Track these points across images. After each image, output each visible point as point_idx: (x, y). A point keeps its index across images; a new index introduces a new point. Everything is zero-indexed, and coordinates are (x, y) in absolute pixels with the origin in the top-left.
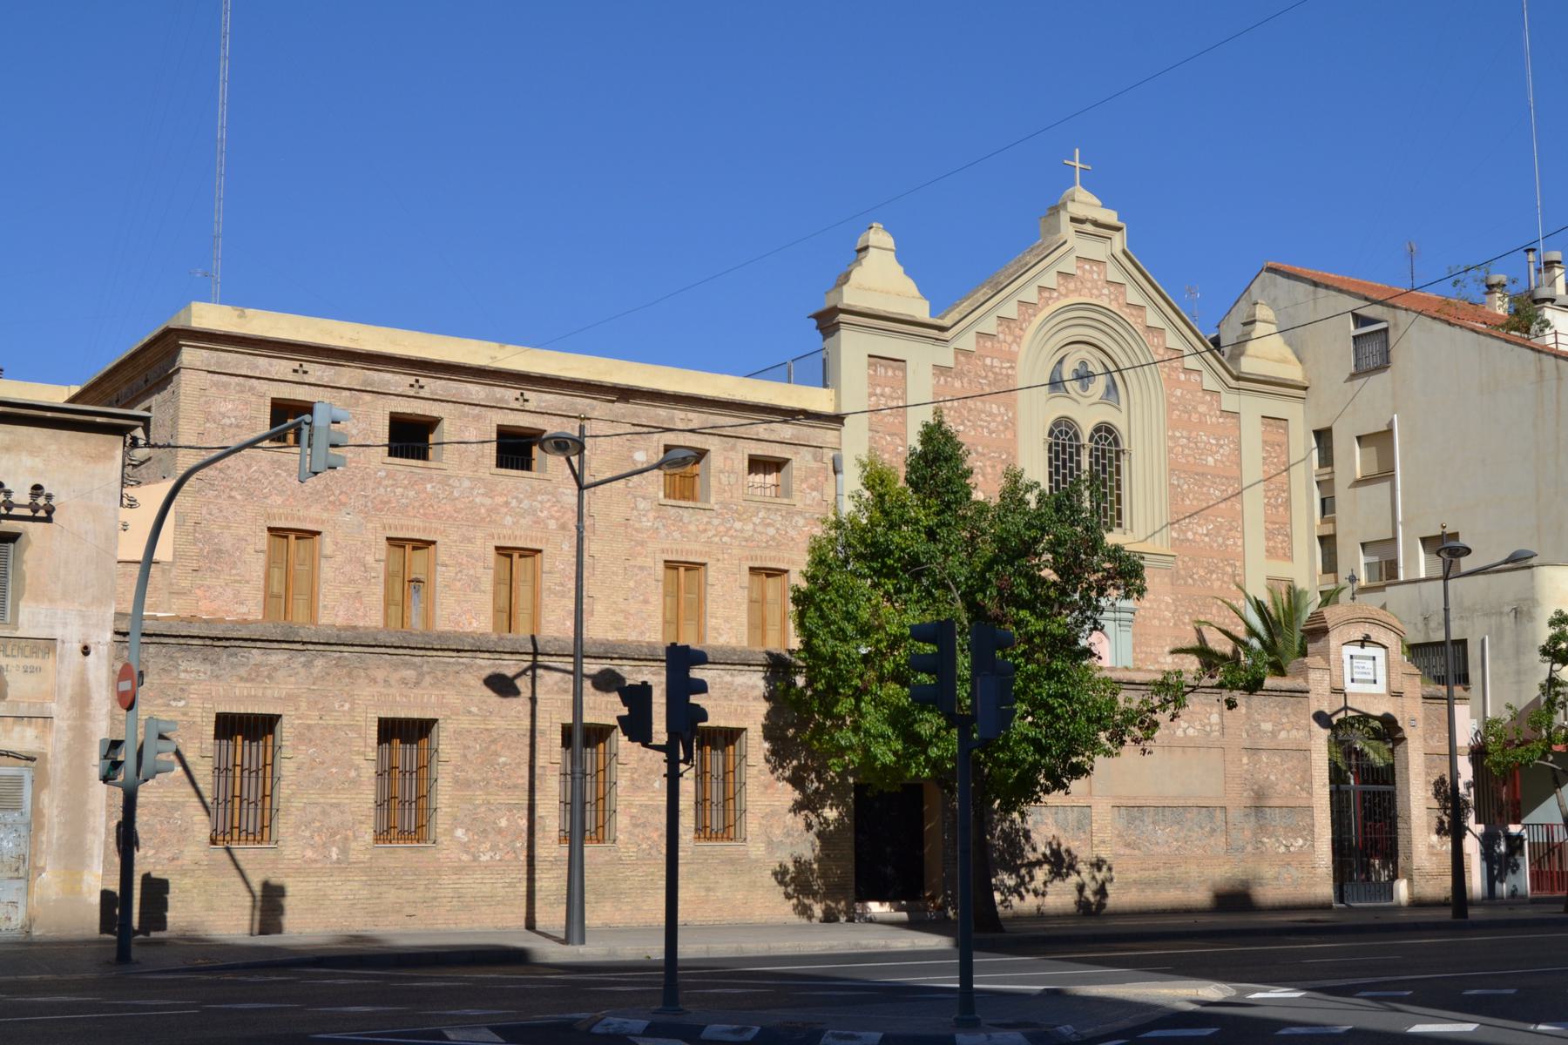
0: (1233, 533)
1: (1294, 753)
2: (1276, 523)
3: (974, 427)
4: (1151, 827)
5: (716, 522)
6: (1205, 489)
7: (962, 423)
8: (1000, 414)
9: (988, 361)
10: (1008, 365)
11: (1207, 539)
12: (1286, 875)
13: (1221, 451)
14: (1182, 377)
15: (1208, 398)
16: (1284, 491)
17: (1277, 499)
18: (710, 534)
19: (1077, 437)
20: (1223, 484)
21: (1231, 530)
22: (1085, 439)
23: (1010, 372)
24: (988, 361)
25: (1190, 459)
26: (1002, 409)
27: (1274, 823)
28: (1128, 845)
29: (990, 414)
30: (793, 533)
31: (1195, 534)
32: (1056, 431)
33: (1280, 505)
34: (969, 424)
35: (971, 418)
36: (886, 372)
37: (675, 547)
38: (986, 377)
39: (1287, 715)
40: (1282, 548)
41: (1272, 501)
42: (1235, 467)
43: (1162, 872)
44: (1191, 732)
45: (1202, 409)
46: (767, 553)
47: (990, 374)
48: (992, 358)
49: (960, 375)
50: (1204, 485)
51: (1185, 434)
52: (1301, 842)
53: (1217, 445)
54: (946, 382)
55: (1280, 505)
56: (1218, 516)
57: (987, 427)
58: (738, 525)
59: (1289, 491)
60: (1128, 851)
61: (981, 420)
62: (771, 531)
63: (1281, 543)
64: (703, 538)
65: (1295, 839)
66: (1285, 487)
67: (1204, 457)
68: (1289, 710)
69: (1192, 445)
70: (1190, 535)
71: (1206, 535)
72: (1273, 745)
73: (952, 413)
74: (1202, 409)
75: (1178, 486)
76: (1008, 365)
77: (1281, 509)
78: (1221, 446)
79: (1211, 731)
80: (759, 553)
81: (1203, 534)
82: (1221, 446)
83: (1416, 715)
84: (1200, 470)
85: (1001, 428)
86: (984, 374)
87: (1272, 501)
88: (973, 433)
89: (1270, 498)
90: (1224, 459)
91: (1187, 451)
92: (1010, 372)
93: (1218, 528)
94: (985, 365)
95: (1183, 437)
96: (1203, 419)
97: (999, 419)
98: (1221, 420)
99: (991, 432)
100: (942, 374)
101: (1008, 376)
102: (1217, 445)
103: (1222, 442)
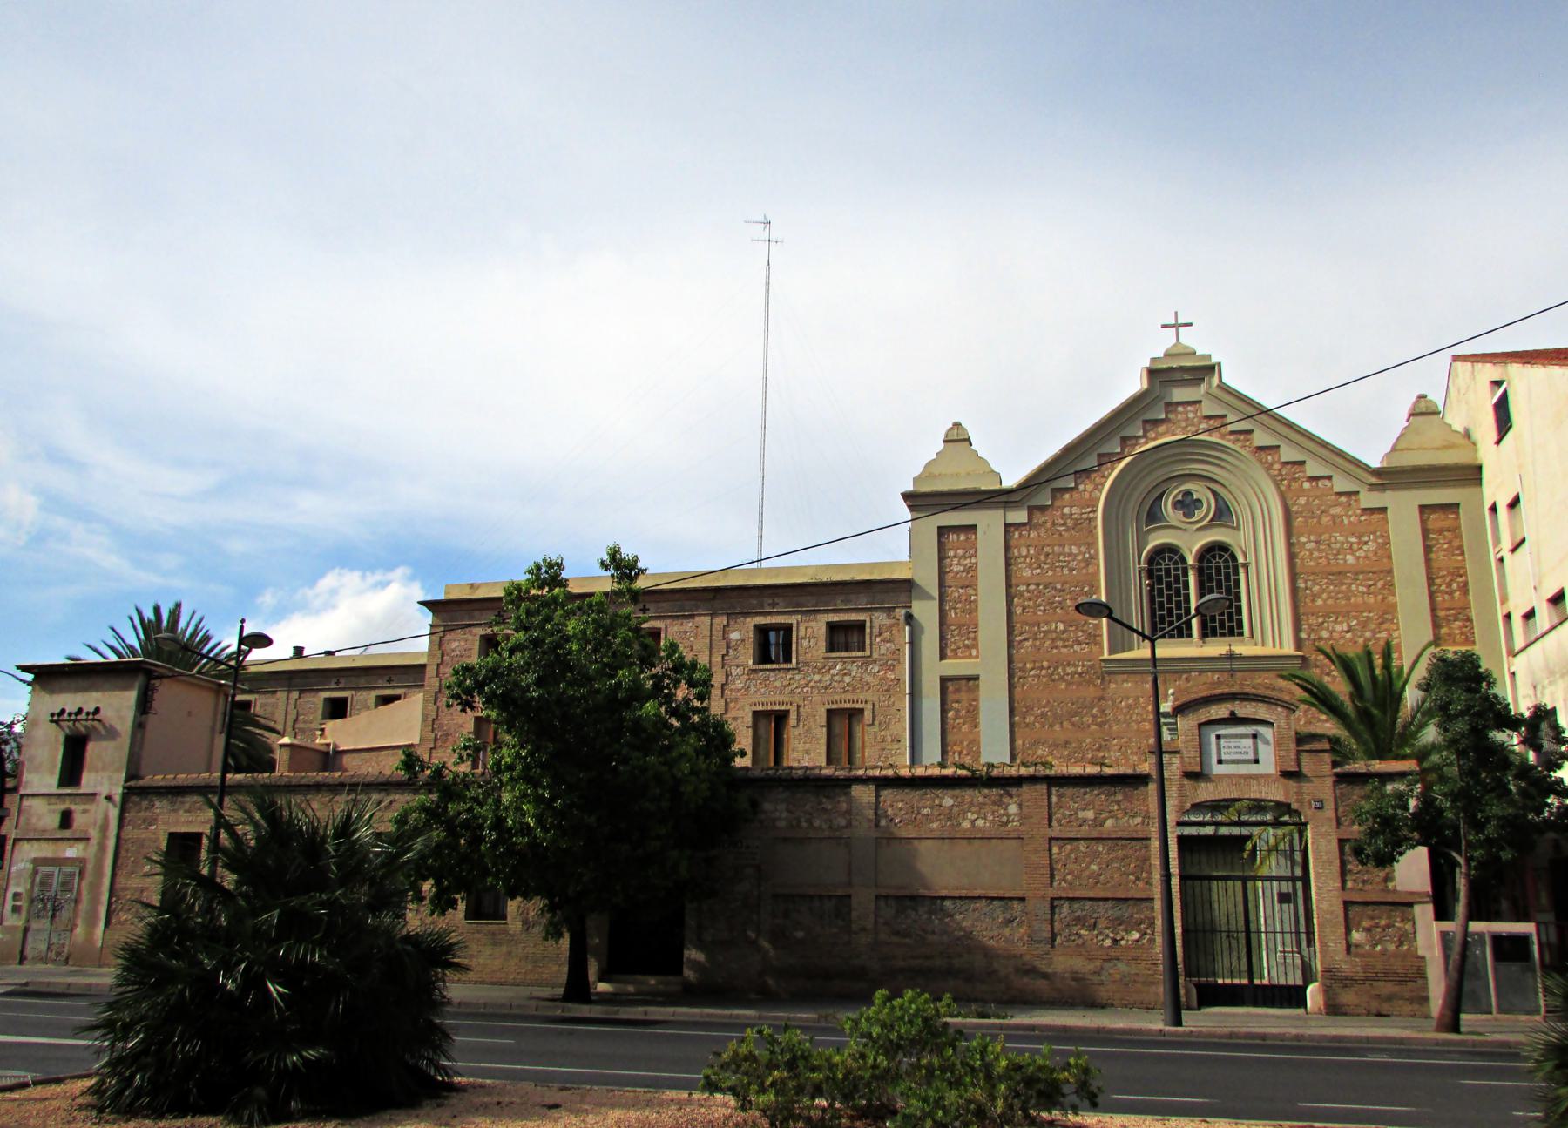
0: (1385, 626)
1: (1124, 842)
2: (1453, 609)
3: (1053, 568)
4: (925, 916)
5: (797, 677)
6: (1344, 587)
7: (1039, 567)
8: (1080, 553)
9: (1066, 511)
10: (1089, 510)
11: (1349, 635)
12: (1111, 971)
13: (1365, 548)
14: (1307, 485)
15: (1343, 499)
16: (1461, 576)
17: (1449, 585)
18: (794, 686)
19: (1183, 560)
20: (1369, 579)
21: (1382, 623)
22: (1190, 561)
23: (1091, 515)
24: (1066, 511)
25: (1323, 561)
26: (1083, 549)
27: (1095, 915)
28: (897, 933)
29: (1070, 554)
30: (868, 678)
31: (1331, 632)
32: (1226, 556)
33: (1455, 591)
34: (1046, 567)
35: (1049, 561)
36: (959, 538)
37: (764, 700)
38: (1063, 525)
39: (1118, 803)
40: (1462, 633)
41: (1443, 587)
42: (1385, 560)
43: (938, 962)
44: (980, 823)
45: (1337, 511)
46: (843, 696)
47: (1069, 521)
48: (1071, 507)
49: (1037, 527)
50: (1343, 584)
51: (1312, 538)
52: (1136, 935)
53: (1358, 543)
54: (1020, 535)
55: (1455, 591)
56: (1363, 612)
57: (1066, 566)
58: (817, 677)
59: (1465, 574)
60: (895, 939)
61: (1060, 561)
62: (847, 679)
63: (1460, 628)
64: (788, 690)
65: (1127, 932)
66: (1462, 572)
67: (1340, 557)
68: (1119, 797)
69: (1321, 547)
70: (1325, 634)
71: (1348, 632)
72: (1095, 834)
73: (1028, 560)
74: (1337, 511)
75: (1306, 588)
76: (1089, 510)
77: (1457, 594)
78: (1366, 543)
79: (1008, 822)
80: (837, 697)
81: (1342, 631)
82: (1366, 543)
83: (1322, 796)
84: (1335, 569)
85: (1083, 564)
86: (1062, 522)
87: (1443, 587)
88: (1050, 573)
89: (1440, 585)
90: (1370, 555)
91: (1316, 554)
92: (1091, 515)
93: (1364, 625)
94: (1063, 516)
95: (1310, 541)
96: (1338, 520)
97: (1080, 558)
98: (1363, 518)
99: (1071, 570)
100: (1017, 530)
101: (1090, 520)
102: (1358, 543)
103: (1366, 539)
